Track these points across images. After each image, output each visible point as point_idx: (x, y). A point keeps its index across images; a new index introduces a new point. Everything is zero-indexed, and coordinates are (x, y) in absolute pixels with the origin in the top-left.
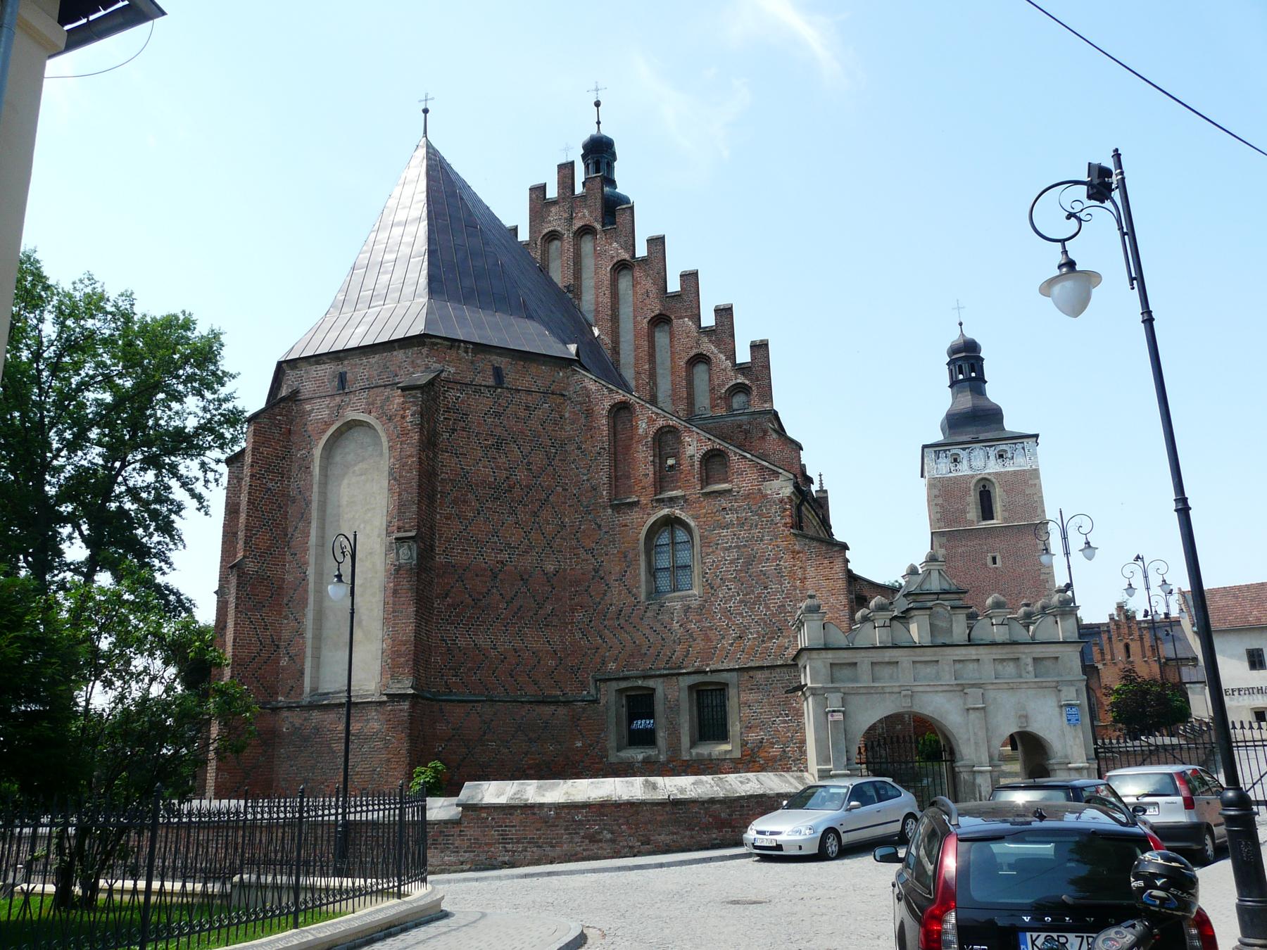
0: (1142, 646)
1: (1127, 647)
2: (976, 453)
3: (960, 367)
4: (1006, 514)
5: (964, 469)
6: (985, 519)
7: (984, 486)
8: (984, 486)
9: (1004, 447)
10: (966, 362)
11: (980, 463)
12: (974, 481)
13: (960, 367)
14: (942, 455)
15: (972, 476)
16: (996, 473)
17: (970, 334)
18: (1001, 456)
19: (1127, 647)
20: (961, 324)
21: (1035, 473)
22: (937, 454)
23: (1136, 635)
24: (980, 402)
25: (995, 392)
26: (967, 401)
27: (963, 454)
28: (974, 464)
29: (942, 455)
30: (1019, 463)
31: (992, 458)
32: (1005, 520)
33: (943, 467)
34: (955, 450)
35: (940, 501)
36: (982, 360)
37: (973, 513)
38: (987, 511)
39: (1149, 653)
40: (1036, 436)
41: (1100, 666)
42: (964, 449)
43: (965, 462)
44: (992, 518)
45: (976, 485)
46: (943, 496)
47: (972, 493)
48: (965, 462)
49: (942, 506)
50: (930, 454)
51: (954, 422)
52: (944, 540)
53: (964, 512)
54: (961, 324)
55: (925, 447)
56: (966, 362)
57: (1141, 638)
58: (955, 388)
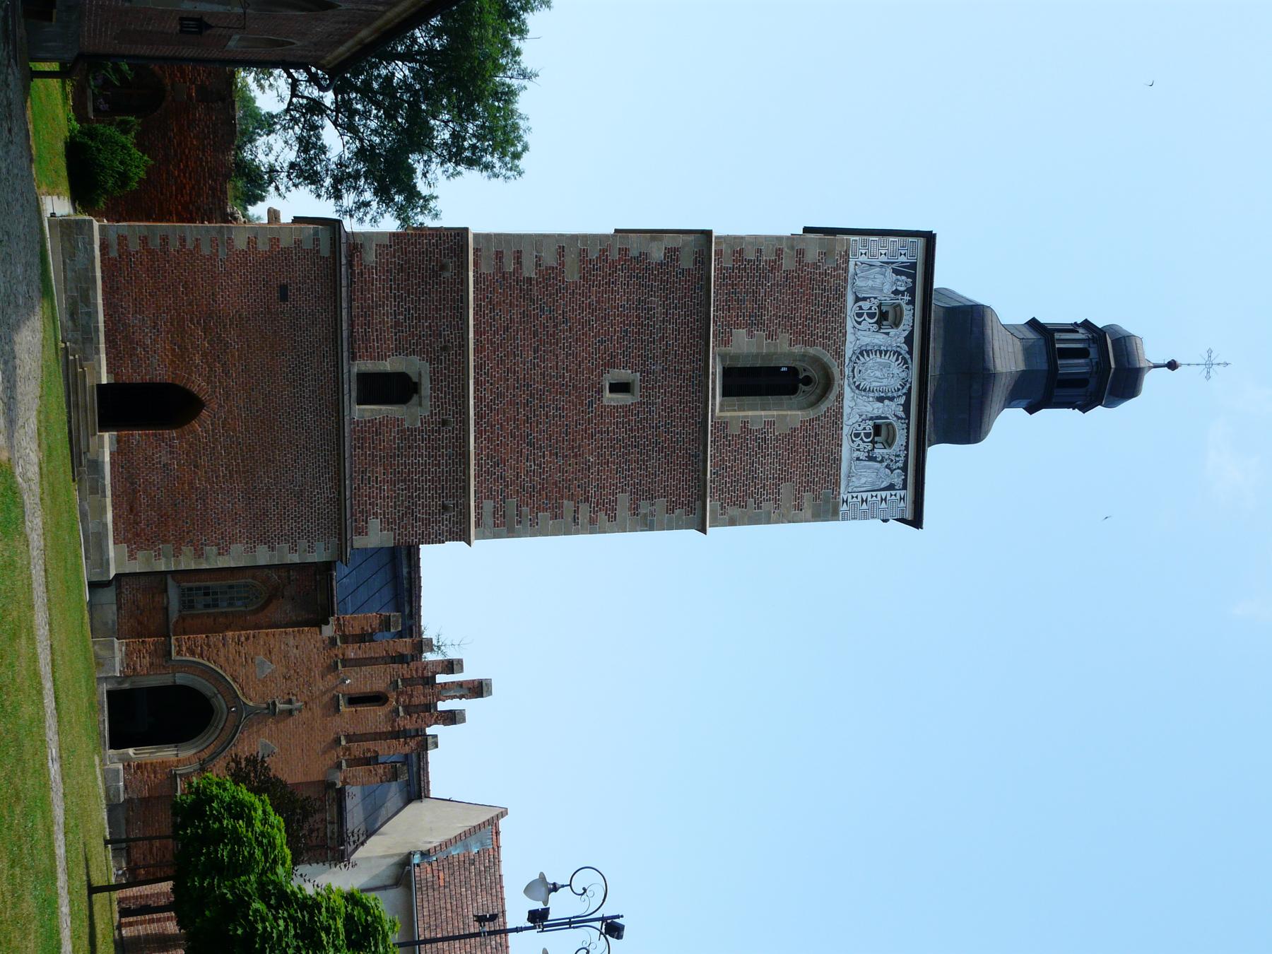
0: (378, 736)
1: (377, 699)
2: (896, 369)
3: (1082, 353)
4: (735, 430)
5: (859, 334)
6: (727, 372)
7: (808, 381)
8: (808, 381)
9: (900, 440)
10: (1087, 368)
11: (873, 375)
12: (827, 357)
13: (1082, 353)
14: (903, 283)
15: (839, 354)
16: (838, 414)
17: (1151, 381)
18: (877, 429)
19: (377, 699)
20: (1172, 365)
21: (828, 510)
22: (906, 270)
23: (405, 722)
24: (1000, 391)
25: (1010, 424)
26: (1007, 359)
27: (896, 337)
28: (873, 361)
29: (903, 283)
30: (858, 472)
31: (877, 409)
32: (722, 425)
33: (874, 280)
34: (910, 317)
35: (788, 263)
36: (1084, 409)
37: (746, 344)
38: (748, 381)
39: (358, 749)
40: (916, 521)
41: (328, 630)
42: (909, 340)
43: (879, 339)
44: (726, 393)
45: (816, 361)
46: (805, 271)
47: (798, 349)
48: (879, 339)
49: (774, 266)
50: (913, 252)
51: (968, 322)
52: (686, 262)
53: (754, 322)
54: (1172, 365)
55: (930, 238)
56: (1087, 368)
57: (396, 734)
58: (1031, 335)
